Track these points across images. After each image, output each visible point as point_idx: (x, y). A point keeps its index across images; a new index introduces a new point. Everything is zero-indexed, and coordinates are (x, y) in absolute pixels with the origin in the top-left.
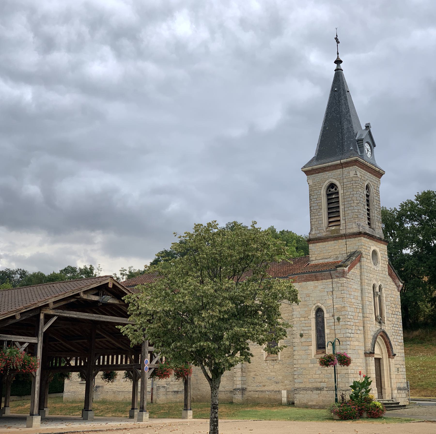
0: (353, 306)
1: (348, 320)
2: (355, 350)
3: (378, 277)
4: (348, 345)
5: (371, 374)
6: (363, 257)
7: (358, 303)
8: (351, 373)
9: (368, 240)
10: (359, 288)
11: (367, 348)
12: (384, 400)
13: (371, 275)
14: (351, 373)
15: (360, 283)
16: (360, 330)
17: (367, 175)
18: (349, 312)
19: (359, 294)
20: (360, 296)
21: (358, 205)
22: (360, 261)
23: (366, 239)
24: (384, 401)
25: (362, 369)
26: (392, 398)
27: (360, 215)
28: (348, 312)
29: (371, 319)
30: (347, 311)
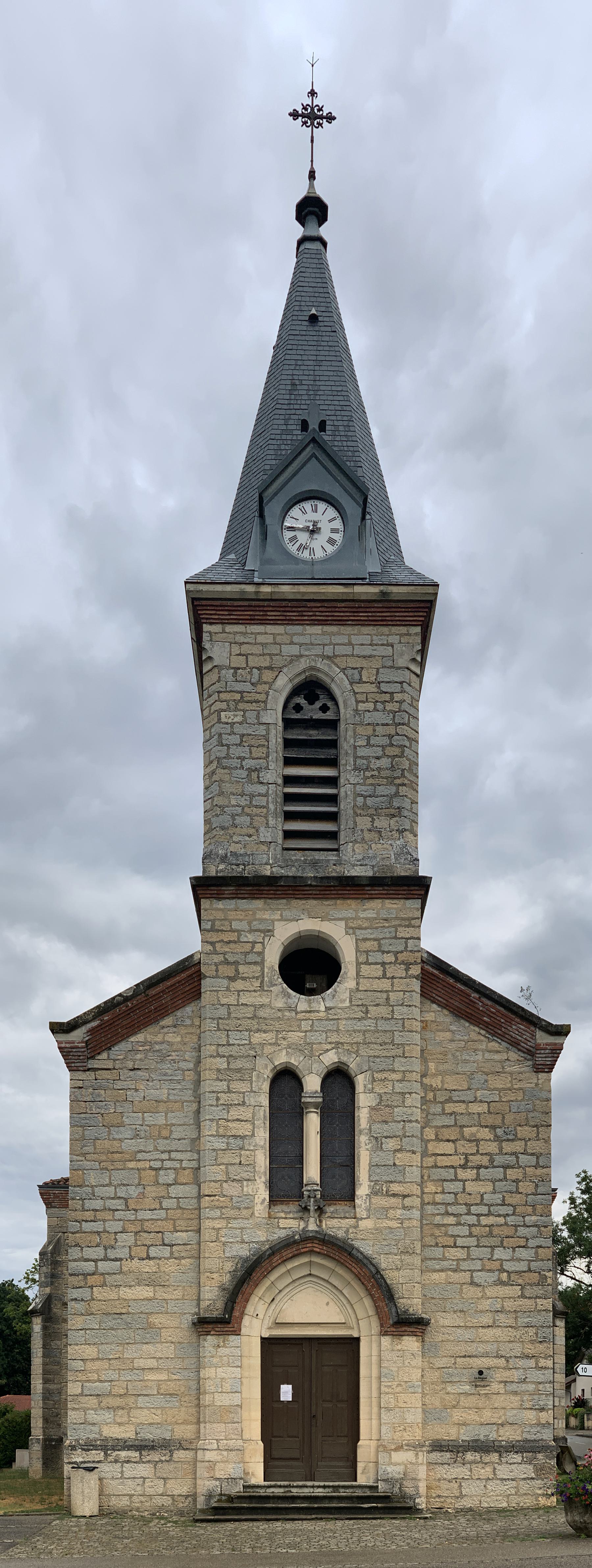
0: (131, 1165)
1: (89, 1215)
2: (123, 1316)
3: (313, 1037)
4: (76, 1299)
5: (206, 1393)
6: (205, 977)
7: (170, 1152)
8: (86, 1392)
9: (259, 903)
10: (188, 1095)
11: (204, 1304)
12: (289, 1486)
13: (257, 1038)
14: (82, 1394)
15: (190, 1076)
16: (172, 1246)
17: (296, 639)
18: (96, 1189)
19: (181, 1117)
20: (192, 1122)
21: (215, 778)
22: (196, 994)
23: (233, 901)
24: (294, 1490)
25: (175, 1377)
26: (377, 1480)
27: (217, 815)
28: (92, 1187)
29: (235, 1199)
30: (78, 1186)
